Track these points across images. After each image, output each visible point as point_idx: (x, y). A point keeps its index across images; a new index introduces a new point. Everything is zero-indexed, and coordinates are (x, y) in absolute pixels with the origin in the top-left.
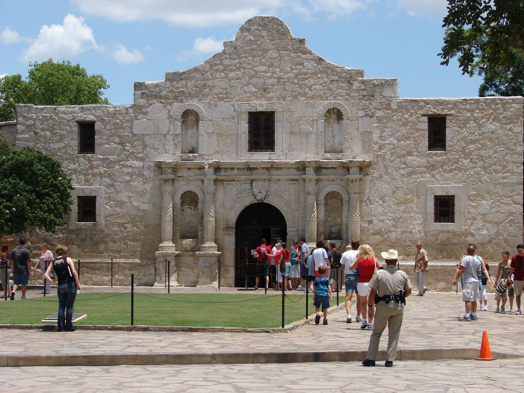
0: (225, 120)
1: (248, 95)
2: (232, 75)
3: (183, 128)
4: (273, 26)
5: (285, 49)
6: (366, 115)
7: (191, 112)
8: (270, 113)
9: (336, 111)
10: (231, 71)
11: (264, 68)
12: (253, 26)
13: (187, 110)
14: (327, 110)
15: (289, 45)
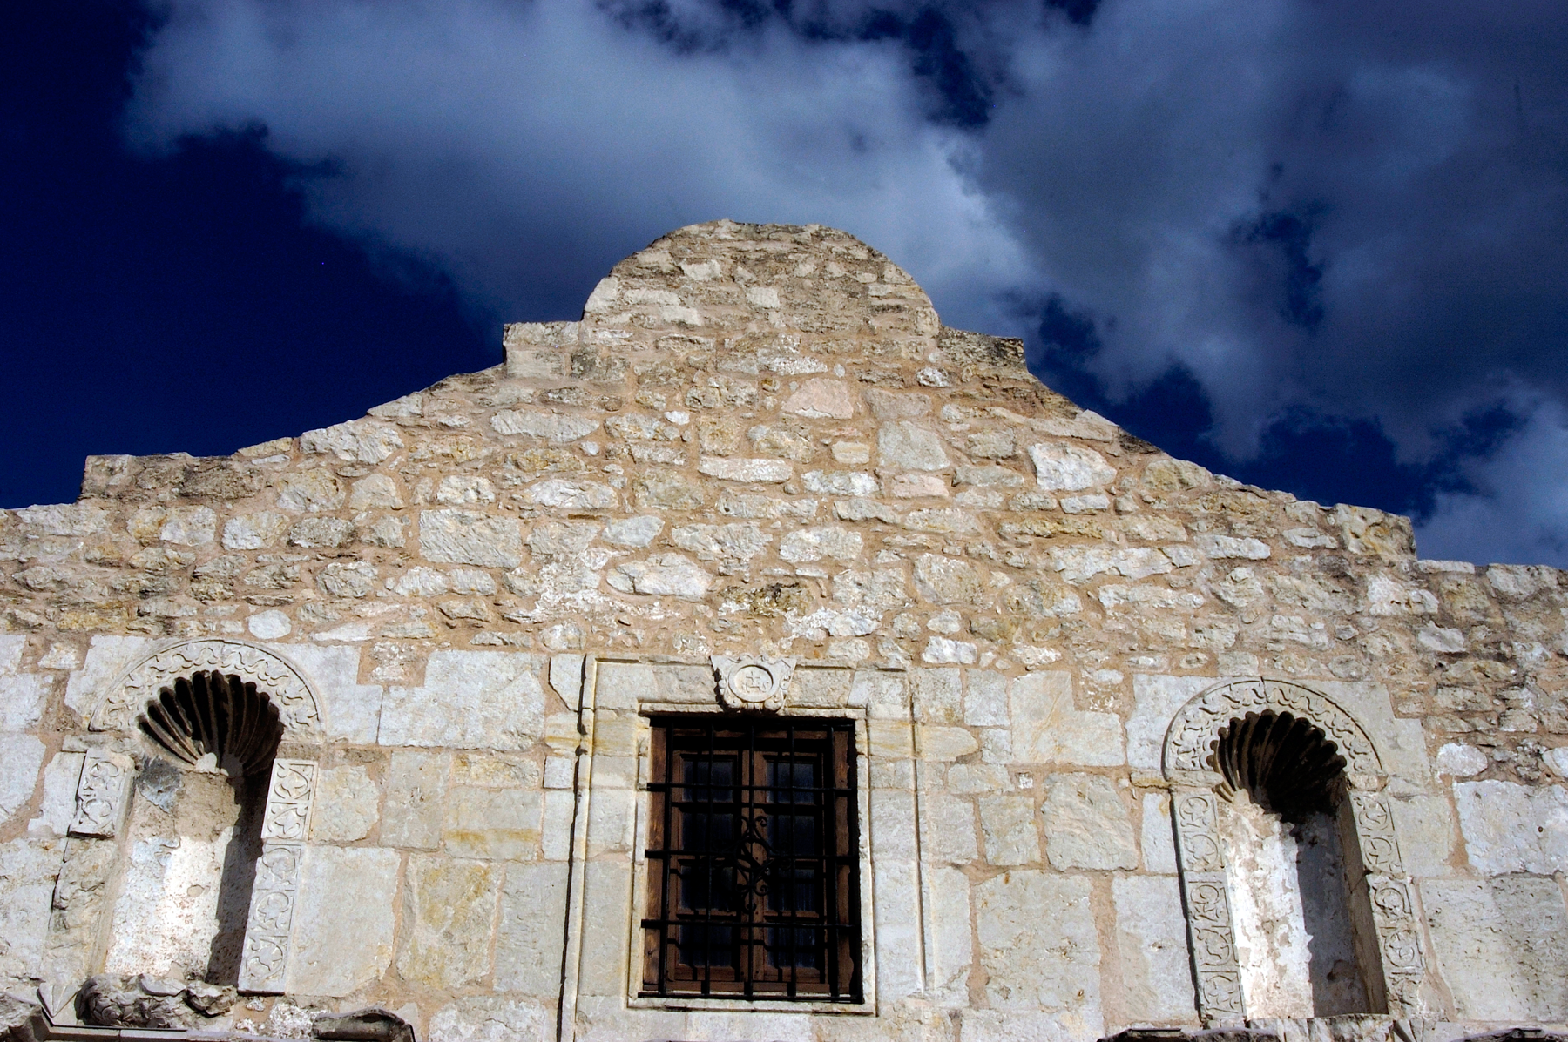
0: (472, 757)
1: (657, 614)
2: (554, 493)
3: (140, 816)
4: (823, 268)
5: (907, 380)
6: (1496, 768)
7: (222, 715)
8: (820, 735)
9: (1265, 752)
10: (551, 467)
11: (765, 469)
12: (699, 261)
13: (198, 676)
14: (1226, 724)
15: (926, 363)
